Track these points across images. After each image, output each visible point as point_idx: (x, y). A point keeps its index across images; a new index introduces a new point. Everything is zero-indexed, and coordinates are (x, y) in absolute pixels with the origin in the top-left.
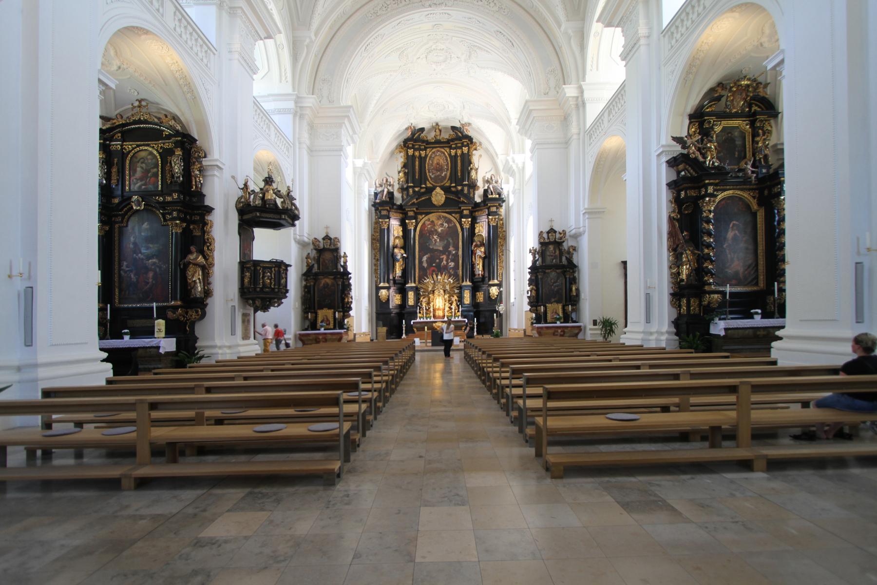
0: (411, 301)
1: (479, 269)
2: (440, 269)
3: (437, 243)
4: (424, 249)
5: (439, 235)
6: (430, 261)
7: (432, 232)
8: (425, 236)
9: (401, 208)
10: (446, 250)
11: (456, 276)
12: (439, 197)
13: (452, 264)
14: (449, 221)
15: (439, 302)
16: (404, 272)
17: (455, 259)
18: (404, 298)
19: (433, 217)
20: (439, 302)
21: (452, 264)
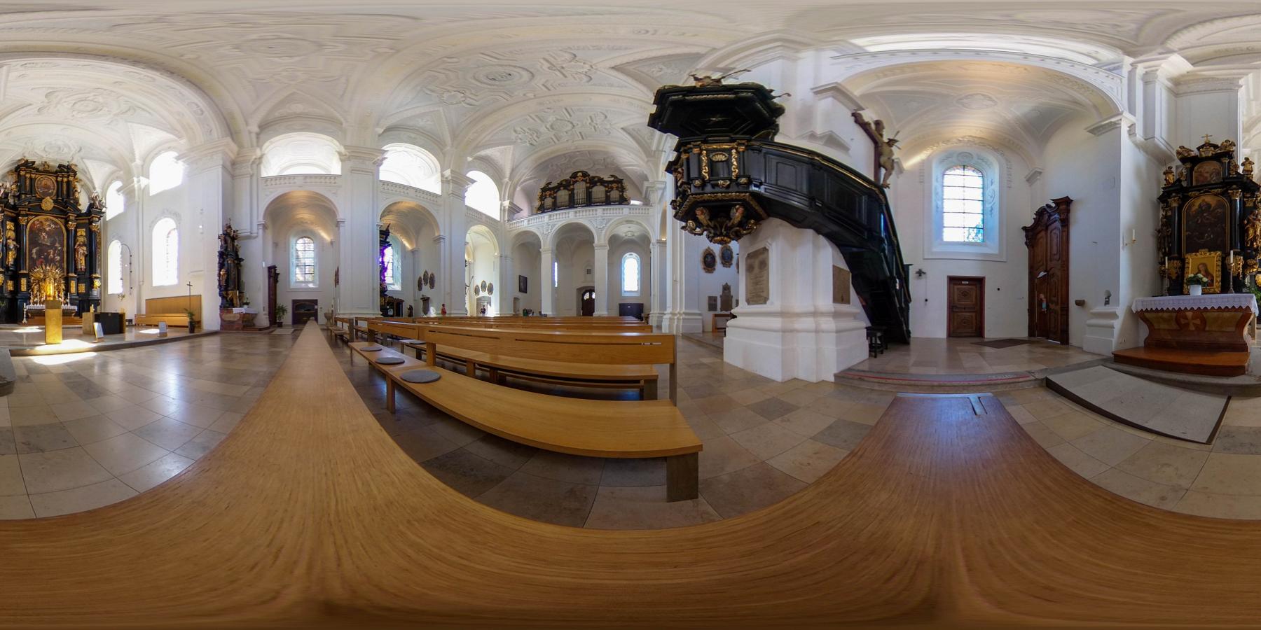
0: (24, 288)
1: (82, 264)
2: (49, 261)
3: (45, 239)
4: (34, 242)
5: (47, 233)
6: (39, 253)
7: (41, 230)
8: (35, 233)
9: (14, 207)
10: (52, 246)
11: (62, 268)
12: (48, 204)
13: (58, 258)
14: (56, 224)
15: (50, 289)
16: (16, 260)
17: (61, 253)
18: (17, 285)
19: (41, 218)
20: (50, 289)
21: (58, 258)
